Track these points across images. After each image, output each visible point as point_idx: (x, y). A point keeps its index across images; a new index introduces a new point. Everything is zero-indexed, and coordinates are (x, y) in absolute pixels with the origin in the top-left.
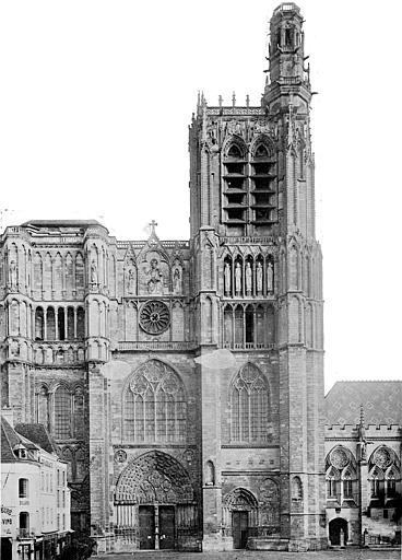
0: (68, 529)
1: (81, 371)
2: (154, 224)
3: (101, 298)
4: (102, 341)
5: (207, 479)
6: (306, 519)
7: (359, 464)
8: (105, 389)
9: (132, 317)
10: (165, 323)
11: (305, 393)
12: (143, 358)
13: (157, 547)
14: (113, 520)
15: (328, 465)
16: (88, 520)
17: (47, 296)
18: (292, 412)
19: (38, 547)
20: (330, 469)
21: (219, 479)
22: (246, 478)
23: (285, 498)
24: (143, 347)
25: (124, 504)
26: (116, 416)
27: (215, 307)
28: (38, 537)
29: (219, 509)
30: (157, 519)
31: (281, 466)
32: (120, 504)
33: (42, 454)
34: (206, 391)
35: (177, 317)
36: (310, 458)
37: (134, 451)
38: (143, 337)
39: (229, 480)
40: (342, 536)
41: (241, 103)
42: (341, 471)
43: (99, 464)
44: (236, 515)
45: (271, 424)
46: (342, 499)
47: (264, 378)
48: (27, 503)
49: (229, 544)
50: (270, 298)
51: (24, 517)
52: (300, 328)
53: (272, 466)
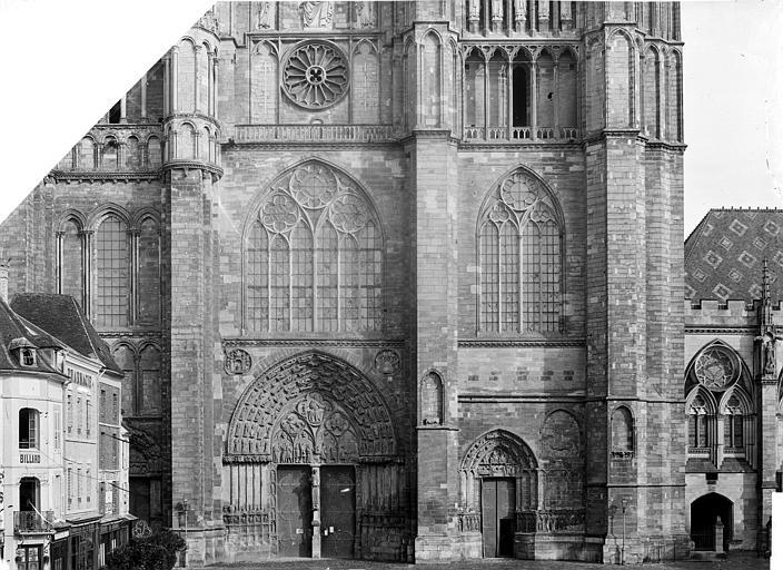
0: (124, 511)
1: (154, 186)
4: (200, 125)
5: (427, 409)
6: (642, 497)
7: (758, 383)
8: (207, 223)
9: (264, 72)
10: (338, 83)
11: (642, 231)
12: (290, 159)
13: (316, 550)
14: (222, 494)
15: (691, 381)
16: (167, 494)
18: (615, 272)
19: (58, 549)
20: (694, 392)
21: (454, 408)
22: (511, 408)
23: (597, 451)
24: (288, 135)
25: (246, 463)
27: (448, 54)
28: (59, 530)
29: (452, 473)
30: (316, 492)
31: (587, 384)
32: (236, 463)
33: (64, 359)
35: (364, 74)
36: (653, 366)
37: (267, 352)
38: (289, 114)
40: (719, 532)
42: (718, 395)
43: (191, 377)
45: (567, 296)
46: (722, 455)
47: (554, 200)
48: (37, 459)
49: (474, 547)
50: (567, 35)
51: (29, 488)
52: (631, 97)
53: (568, 384)
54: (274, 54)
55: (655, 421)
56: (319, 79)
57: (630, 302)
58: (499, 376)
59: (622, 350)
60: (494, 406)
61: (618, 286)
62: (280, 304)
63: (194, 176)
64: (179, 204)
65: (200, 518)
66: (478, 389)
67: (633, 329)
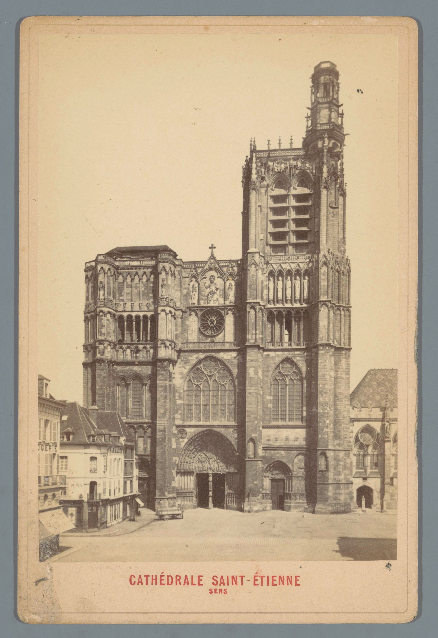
2: (212, 247)
3: (168, 309)
4: (168, 343)
5: (250, 452)
6: (331, 488)
7: (384, 442)
8: (170, 381)
12: (202, 356)
14: (175, 484)
17: (136, 308)
18: (321, 399)
21: (260, 452)
22: (283, 452)
26: (179, 402)
34: (250, 382)
39: (269, 454)
41: (286, 145)
43: (164, 439)
44: (275, 483)
46: (369, 471)
54: (197, 315)
55: (337, 458)
56: (213, 324)
57: (326, 411)
58: (278, 440)
59: (323, 430)
60: (276, 451)
61: (322, 405)
62: (198, 412)
63: (165, 363)
64: (161, 374)
65: (166, 493)
66: (270, 445)
67: (327, 422)
